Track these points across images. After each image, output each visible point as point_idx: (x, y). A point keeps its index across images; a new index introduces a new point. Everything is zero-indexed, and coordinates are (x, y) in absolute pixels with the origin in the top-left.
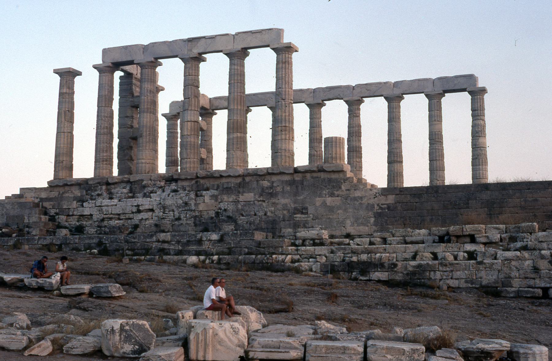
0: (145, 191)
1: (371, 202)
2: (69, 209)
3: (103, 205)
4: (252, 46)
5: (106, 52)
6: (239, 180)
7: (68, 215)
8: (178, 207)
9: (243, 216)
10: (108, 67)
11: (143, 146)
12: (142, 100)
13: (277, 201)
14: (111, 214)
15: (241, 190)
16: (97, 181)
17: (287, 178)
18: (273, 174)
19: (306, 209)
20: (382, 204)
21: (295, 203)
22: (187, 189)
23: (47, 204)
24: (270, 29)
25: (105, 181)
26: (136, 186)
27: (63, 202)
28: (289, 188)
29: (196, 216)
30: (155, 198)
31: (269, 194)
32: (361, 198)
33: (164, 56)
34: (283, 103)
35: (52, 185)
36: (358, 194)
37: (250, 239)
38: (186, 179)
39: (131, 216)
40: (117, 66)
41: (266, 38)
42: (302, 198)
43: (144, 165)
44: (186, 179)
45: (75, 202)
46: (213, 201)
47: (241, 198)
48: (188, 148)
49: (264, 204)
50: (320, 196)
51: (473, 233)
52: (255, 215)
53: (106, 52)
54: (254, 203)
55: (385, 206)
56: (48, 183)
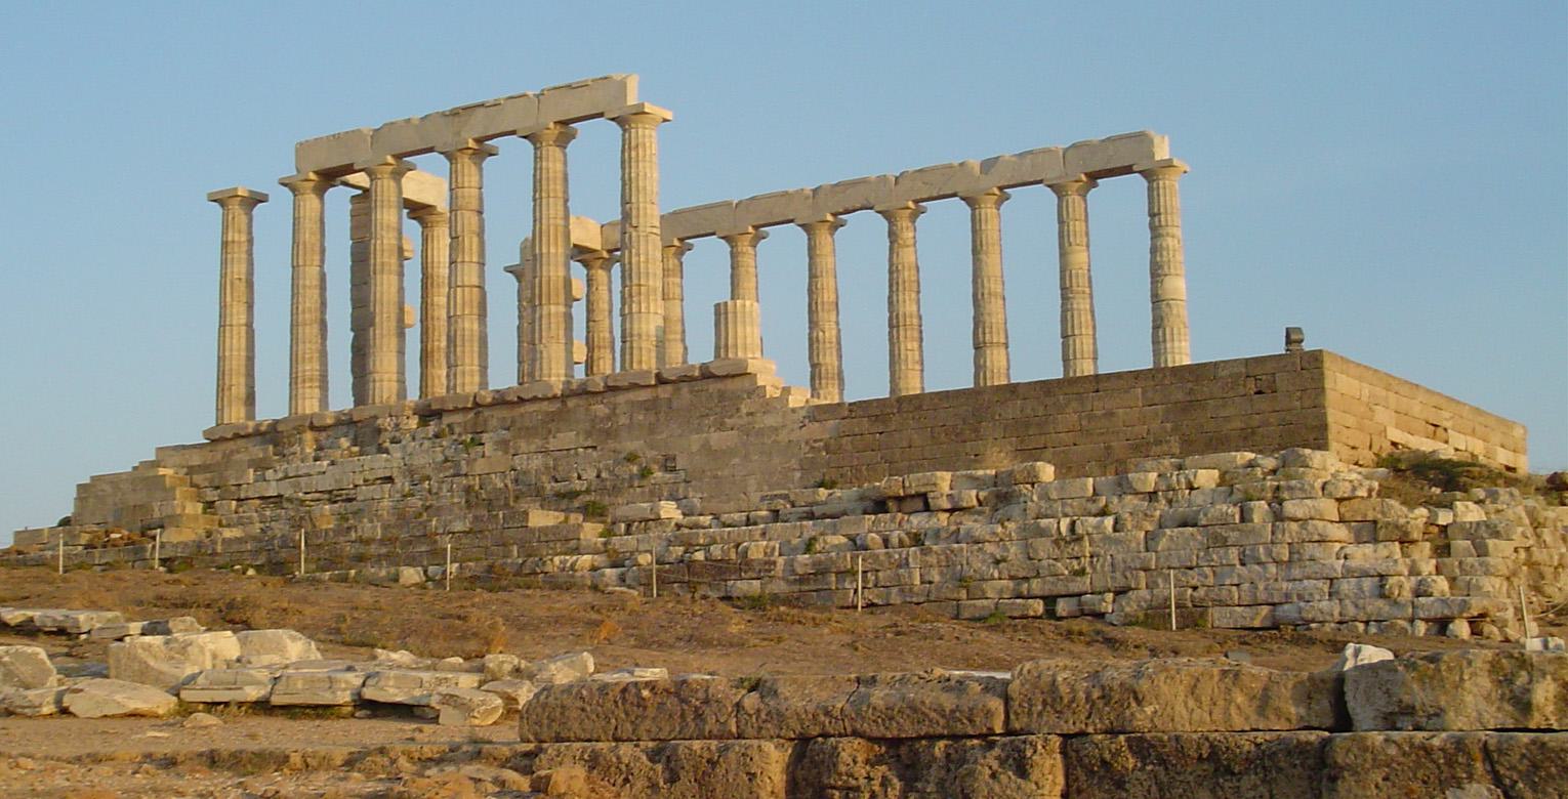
1: (793, 437)
3: (300, 473)
5: (302, 149)
9: (557, 481)
13: (618, 447)
14: (316, 492)
16: (291, 425)
17: (643, 395)
20: (815, 441)
23: (198, 478)
28: (641, 417)
32: (775, 429)
33: (409, 150)
34: (634, 234)
35: (214, 440)
36: (770, 421)
38: (456, 410)
40: (330, 177)
42: (664, 436)
44: (456, 410)
47: (553, 444)
50: (699, 431)
51: (923, 490)
53: (302, 149)
55: (822, 444)
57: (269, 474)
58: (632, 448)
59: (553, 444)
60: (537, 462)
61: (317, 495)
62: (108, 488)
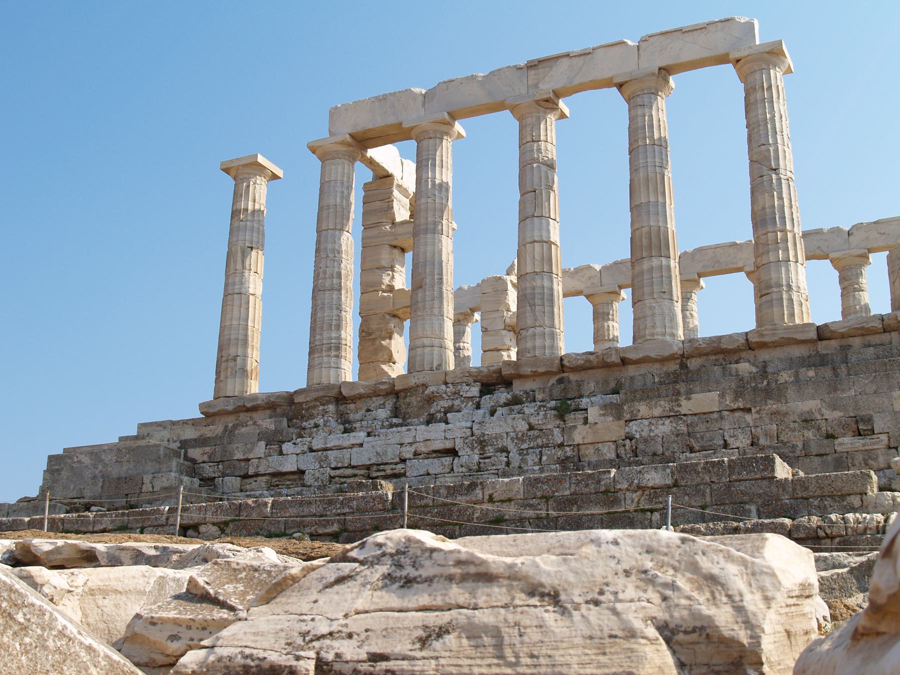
0: (432, 411)
2: (249, 460)
3: (328, 445)
4: (685, 58)
6: (673, 367)
7: (246, 476)
8: (520, 439)
9: (692, 450)
10: (342, 143)
11: (424, 308)
12: (423, 206)
14: (351, 466)
15: (682, 387)
16: (314, 395)
18: (763, 345)
19: (869, 420)
21: (834, 407)
22: (539, 396)
23: (195, 453)
24: (728, 20)
25: (334, 393)
26: (407, 400)
27: (235, 446)
29: (567, 458)
30: (459, 424)
31: (761, 389)
34: (774, 176)
35: (210, 414)
37: (763, 478)
38: (535, 375)
39: (399, 468)
41: (718, 43)
43: (427, 350)
45: (262, 444)
46: (611, 419)
47: (686, 406)
48: (538, 301)
49: (748, 418)
52: (726, 445)
53: (334, 113)
54: (722, 418)
56: (203, 407)
57: (287, 447)
58: (806, 409)
59: (686, 406)
60: (665, 428)
61: (349, 472)
62: (86, 460)
